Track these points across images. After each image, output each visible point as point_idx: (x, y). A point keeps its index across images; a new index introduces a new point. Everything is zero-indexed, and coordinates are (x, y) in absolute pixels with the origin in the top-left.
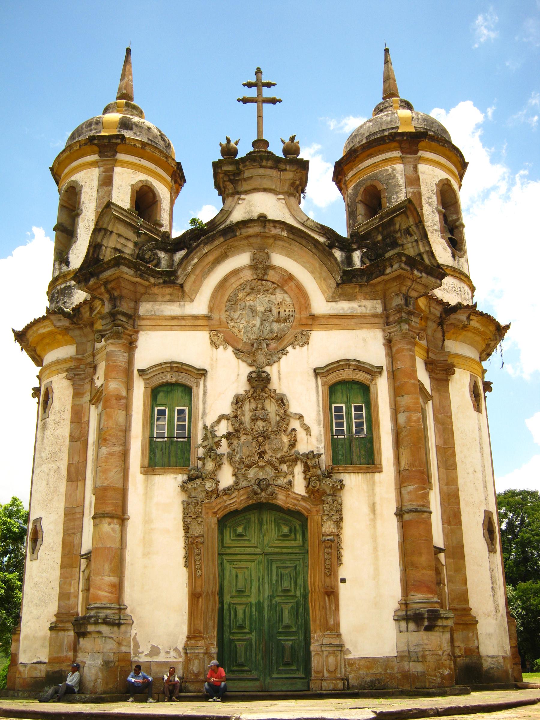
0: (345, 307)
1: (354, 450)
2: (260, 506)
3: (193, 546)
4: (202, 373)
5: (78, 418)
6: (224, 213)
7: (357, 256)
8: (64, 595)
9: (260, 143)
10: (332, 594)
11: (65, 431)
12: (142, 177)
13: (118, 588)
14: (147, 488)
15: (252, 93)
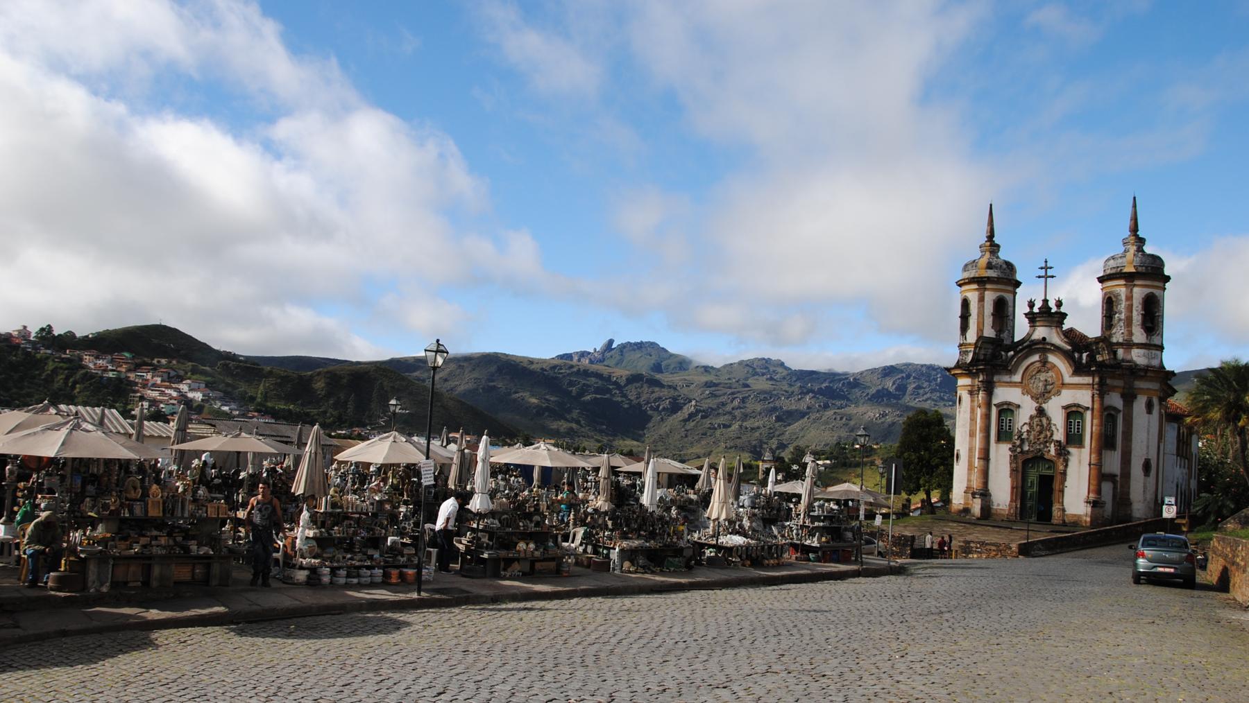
0: (1077, 380)
1: (1074, 438)
2: (1038, 458)
3: (1014, 471)
4: (1019, 406)
5: (973, 411)
6: (1029, 335)
7: (1084, 355)
8: (969, 481)
9: (1046, 301)
10: (1062, 491)
11: (968, 416)
12: (999, 294)
13: (986, 483)
14: (997, 451)
15: (1042, 273)
